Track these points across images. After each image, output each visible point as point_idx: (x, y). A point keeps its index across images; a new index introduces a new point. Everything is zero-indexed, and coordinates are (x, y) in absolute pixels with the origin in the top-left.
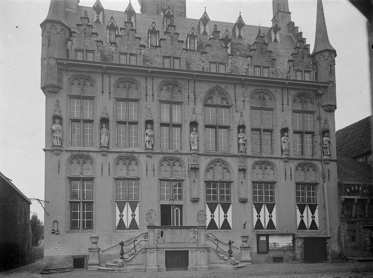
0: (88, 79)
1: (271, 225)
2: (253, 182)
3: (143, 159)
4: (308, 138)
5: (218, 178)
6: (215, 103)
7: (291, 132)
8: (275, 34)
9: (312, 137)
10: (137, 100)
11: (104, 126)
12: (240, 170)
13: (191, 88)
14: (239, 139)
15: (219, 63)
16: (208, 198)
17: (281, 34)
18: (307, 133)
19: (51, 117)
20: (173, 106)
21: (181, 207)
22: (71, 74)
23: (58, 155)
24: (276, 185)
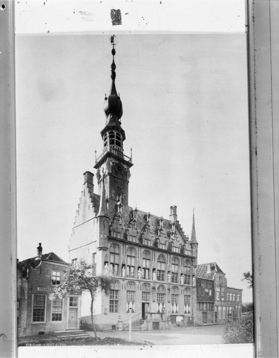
0: (118, 245)
1: (177, 312)
2: (157, 294)
3: (137, 283)
4: (116, 266)
5: (161, 292)
6: (160, 261)
7: (184, 274)
8: (120, 208)
9: (118, 266)
10: (134, 257)
11: (124, 267)
12: (168, 289)
13: (154, 254)
14: (168, 276)
15: (163, 244)
16: (158, 300)
17: (122, 209)
18: (132, 267)
19: (104, 261)
20: (162, 263)
21: (148, 303)
22: (111, 242)
23: (182, 287)
24: (119, 292)
